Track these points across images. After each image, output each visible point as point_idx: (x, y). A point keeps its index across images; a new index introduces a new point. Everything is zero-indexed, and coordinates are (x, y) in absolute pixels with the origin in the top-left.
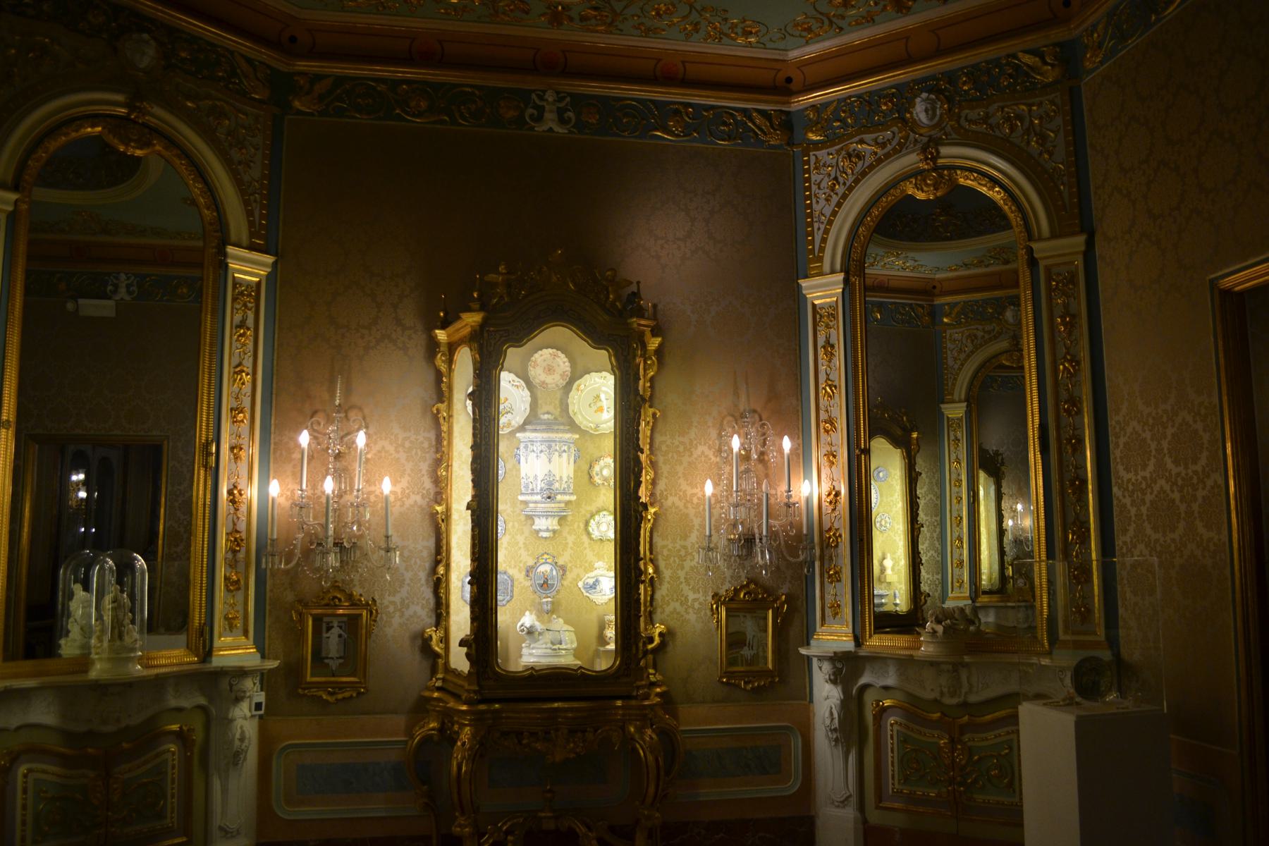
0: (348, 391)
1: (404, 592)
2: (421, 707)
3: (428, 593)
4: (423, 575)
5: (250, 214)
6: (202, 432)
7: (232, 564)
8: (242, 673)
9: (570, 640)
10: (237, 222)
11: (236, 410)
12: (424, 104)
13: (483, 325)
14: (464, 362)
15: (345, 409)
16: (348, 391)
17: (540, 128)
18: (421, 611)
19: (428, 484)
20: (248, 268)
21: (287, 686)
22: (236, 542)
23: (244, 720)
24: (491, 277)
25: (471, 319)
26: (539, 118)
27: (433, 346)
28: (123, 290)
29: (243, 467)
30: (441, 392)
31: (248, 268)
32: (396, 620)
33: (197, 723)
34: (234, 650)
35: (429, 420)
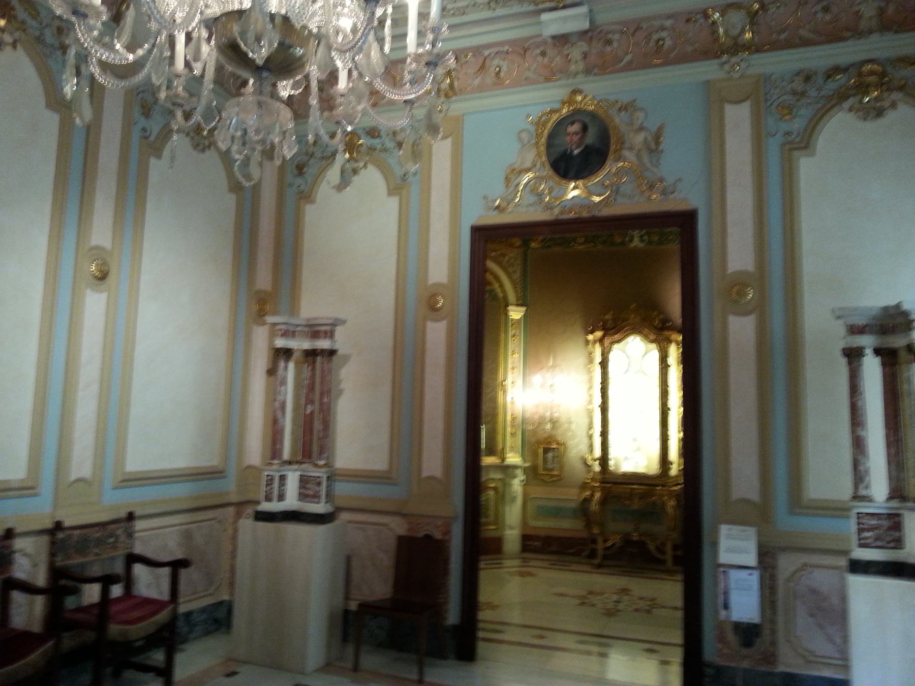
2: (584, 486)
7: (513, 426)
8: (515, 467)
9: (645, 463)
10: (512, 297)
11: (513, 369)
12: (583, 240)
13: (604, 336)
14: (598, 350)
15: (554, 367)
17: (633, 245)
18: (583, 448)
20: (516, 314)
21: (533, 474)
22: (514, 419)
23: (517, 484)
25: (599, 334)
26: (631, 240)
30: (591, 361)
31: (516, 314)
34: (513, 458)
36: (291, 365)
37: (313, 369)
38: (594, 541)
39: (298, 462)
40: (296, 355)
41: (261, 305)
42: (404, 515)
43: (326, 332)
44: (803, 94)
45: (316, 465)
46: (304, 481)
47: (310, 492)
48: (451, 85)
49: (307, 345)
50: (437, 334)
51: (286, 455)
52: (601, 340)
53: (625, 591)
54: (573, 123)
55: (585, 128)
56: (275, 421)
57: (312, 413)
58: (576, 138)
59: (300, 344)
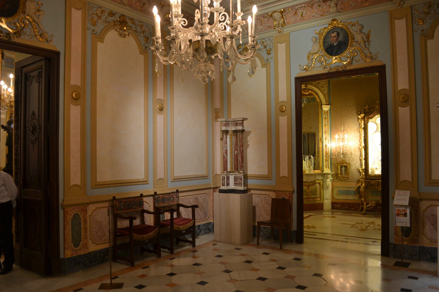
0: (344, 128)
1: (355, 162)
2: (358, 181)
3: (359, 162)
4: (358, 159)
5: (325, 99)
6: (320, 136)
7: (326, 157)
8: (328, 174)
10: (324, 101)
11: (325, 132)
13: (364, 116)
15: (343, 131)
16: (344, 128)
18: (358, 165)
19: (359, 143)
20: (326, 108)
21: (336, 176)
22: (327, 154)
23: (329, 182)
24: (366, 107)
25: (362, 115)
27: (358, 118)
28: (305, 101)
29: (327, 141)
31: (326, 108)
32: (354, 166)
33: (322, 182)
34: (327, 170)
35: (358, 132)
36: (228, 136)
37: (237, 137)
38: (363, 204)
39: (233, 172)
40: (230, 133)
41: (217, 114)
42: (274, 191)
43: (240, 123)
44: (428, 13)
45: (239, 173)
46: (236, 179)
47: (238, 183)
48: (284, 22)
49: (234, 129)
50: (283, 120)
51: (229, 170)
52: (363, 118)
53: (373, 223)
54: (333, 33)
55: (338, 34)
56: (224, 157)
57: (237, 153)
58: (335, 38)
59: (232, 128)
